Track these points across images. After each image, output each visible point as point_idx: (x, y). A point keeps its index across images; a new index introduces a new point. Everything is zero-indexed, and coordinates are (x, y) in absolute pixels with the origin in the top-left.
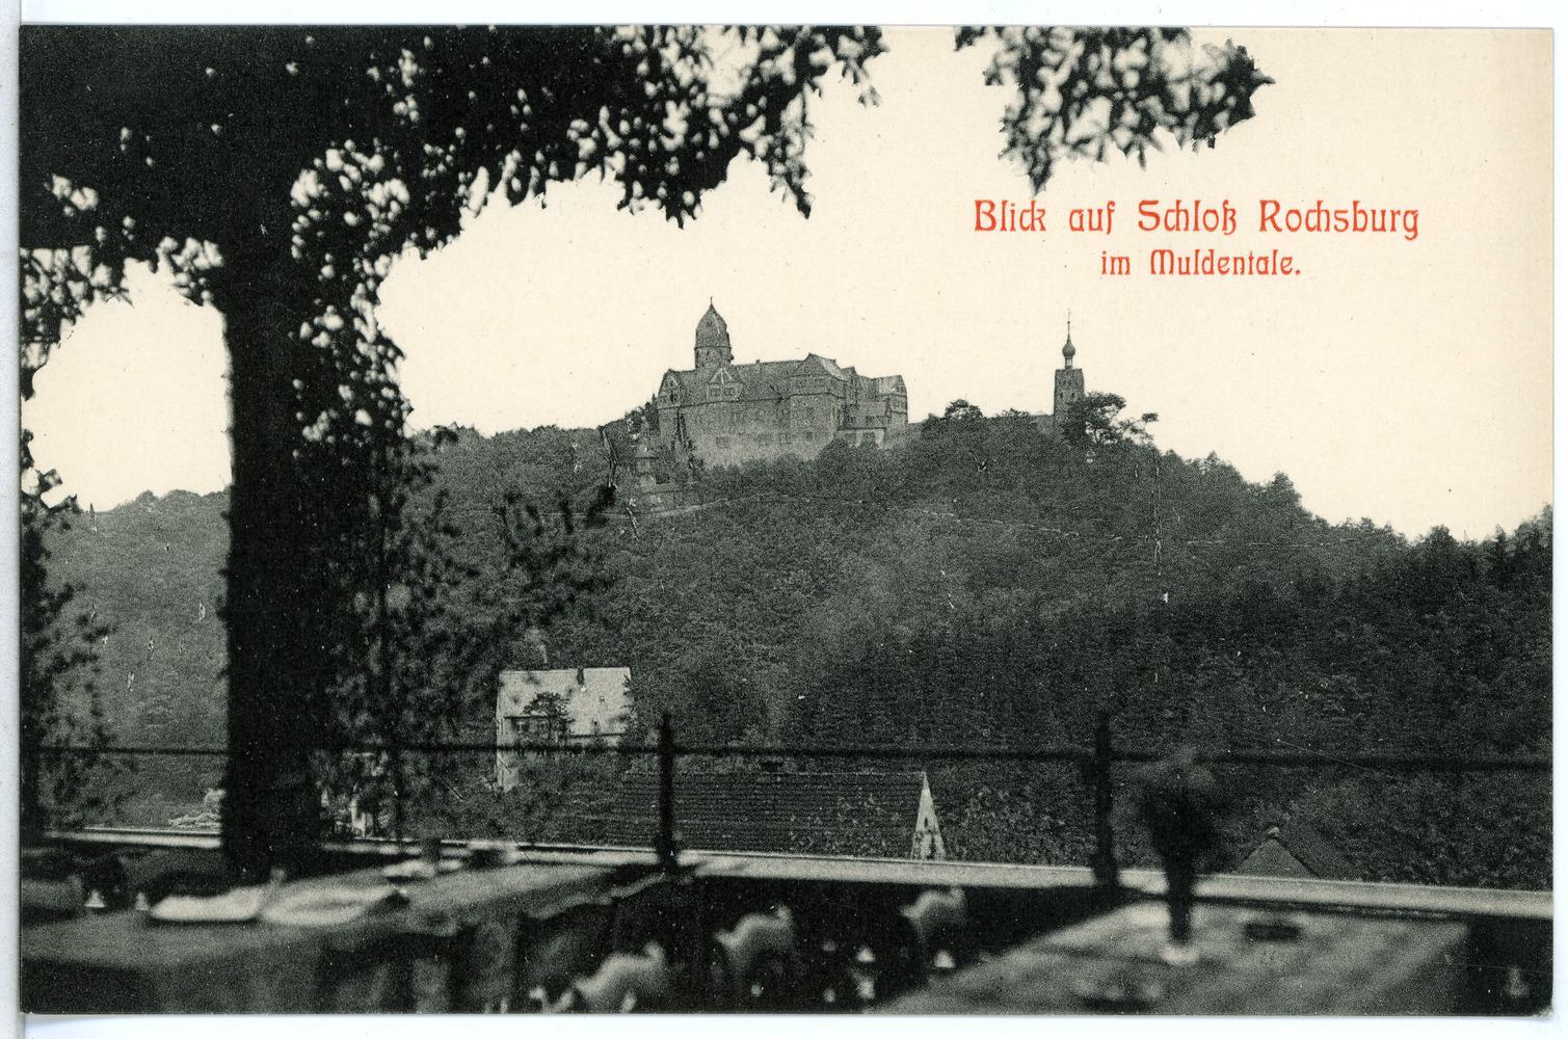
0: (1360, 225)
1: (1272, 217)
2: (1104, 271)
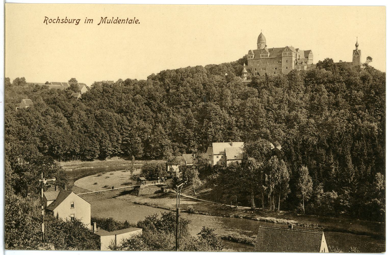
0: (66, 21)
1: (46, 20)
2: (85, 23)
